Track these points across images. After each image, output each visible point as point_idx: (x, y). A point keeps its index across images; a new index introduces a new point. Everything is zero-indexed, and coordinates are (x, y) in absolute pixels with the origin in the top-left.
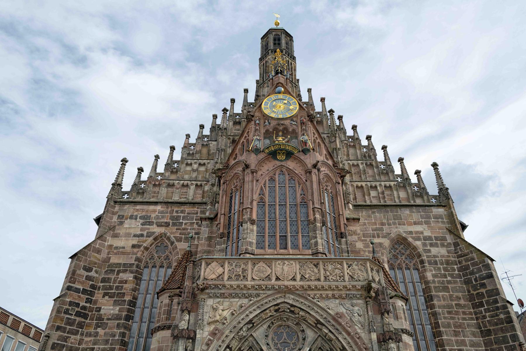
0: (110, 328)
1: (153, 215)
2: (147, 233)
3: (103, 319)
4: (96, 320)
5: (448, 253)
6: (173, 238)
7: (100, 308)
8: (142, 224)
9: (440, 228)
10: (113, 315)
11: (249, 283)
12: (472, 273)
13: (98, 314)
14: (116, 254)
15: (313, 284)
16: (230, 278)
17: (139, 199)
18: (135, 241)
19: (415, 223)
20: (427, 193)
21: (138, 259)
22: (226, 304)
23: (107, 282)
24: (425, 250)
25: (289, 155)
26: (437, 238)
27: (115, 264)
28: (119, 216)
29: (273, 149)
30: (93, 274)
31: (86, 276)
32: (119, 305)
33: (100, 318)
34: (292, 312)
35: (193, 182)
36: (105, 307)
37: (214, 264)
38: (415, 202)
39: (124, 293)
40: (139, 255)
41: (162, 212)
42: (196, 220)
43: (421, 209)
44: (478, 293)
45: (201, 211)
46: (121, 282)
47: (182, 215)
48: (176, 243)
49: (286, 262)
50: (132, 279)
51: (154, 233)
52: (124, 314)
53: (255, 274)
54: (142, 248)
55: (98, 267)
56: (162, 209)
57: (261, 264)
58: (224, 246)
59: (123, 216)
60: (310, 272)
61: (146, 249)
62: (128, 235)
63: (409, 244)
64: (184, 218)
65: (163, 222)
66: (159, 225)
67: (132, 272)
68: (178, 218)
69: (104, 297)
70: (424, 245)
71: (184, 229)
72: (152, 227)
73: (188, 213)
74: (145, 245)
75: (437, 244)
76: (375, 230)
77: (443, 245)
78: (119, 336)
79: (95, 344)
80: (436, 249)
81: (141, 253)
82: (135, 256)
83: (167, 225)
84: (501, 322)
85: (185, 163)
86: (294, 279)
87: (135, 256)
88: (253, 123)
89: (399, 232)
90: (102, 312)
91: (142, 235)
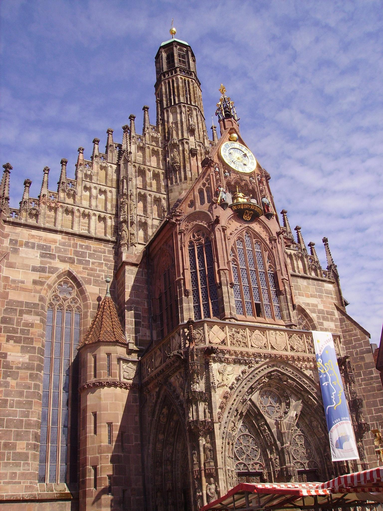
0: (22, 378)
1: (53, 247)
3: (12, 368)
4: (3, 368)
5: (336, 327)
6: (81, 279)
7: (6, 354)
9: (330, 304)
10: (23, 363)
11: (251, 351)
12: (354, 347)
13: (4, 361)
14: (14, 289)
15: (301, 355)
16: (232, 344)
17: (32, 221)
18: (36, 276)
19: (312, 296)
20: (320, 268)
21: (42, 299)
22: (230, 368)
23: (9, 323)
24: (319, 322)
25: (255, 217)
26: (328, 313)
27: (15, 301)
28: (11, 240)
29: (242, 208)
32: (29, 352)
33: (7, 366)
34: (280, 379)
35: (95, 212)
36: (13, 354)
37: (216, 328)
38: (311, 274)
39: (32, 339)
40: (43, 293)
41: (64, 244)
42: (104, 260)
43: (316, 282)
44: (358, 365)
45: (109, 251)
46: (26, 325)
49: (277, 332)
50: (39, 322)
51: (57, 269)
52: (36, 363)
53: (256, 342)
54: (45, 286)
56: (63, 240)
57: (257, 332)
58: (192, 305)
59: (16, 241)
60: (297, 344)
61: (50, 287)
62: (25, 267)
63: (306, 315)
64: (90, 256)
66: (63, 260)
67: (37, 314)
68: (83, 255)
69: (8, 341)
70: (318, 318)
71: (92, 269)
72: (52, 261)
73: (94, 251)
74: (49, 282)
75: (327, 317)
77: (332, 320)
78: (35, 388)
79: (7, 395)
80: (327, 322)
81: (45, 292)
82: (38, 295)
83: (71, 261)
84: (373, 389)
85: (83, 185)
86: (286, 350)
88: (212, 169)
89: (299, 302)
90: (9, 358)
91: (42, 270)
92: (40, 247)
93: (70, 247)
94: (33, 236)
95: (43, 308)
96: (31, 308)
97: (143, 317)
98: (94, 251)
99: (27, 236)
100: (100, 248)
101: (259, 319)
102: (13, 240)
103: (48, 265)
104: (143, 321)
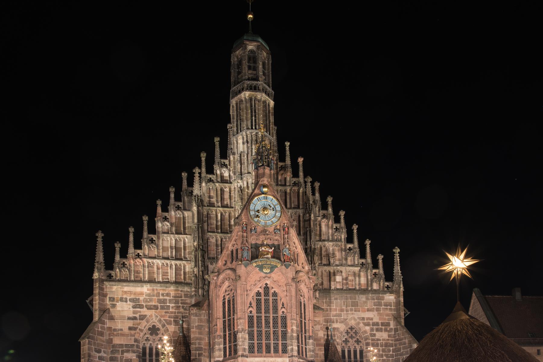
1: (141, 298)
2: (140, 316)
6: (164, 321)
8: (134, 307)
14: (116, 336)
18: (130, 323)
30: (102, 354)
31: (99, 357)
41: (149, 295)
42: (181, 303)
45: (185, 294)
47: (168, 298)
48: (167, 326)
51: (145, 316)
54: (138, 330)
55: (105, 348)
59: (114, 298)
61: (141, 330)
64: (170, 301)
65: (151, 305)
66: (149, 308)
68: (164, 301)
71: (172, 313)
76: (335, 316)
82: (133, 338)
83: (156, 308)
87: (133, 338)
92: (132, 300)
93: (154, 296)
94: (126, 292)
95: (138, 347)
96: (128, 348)
97: (205, 349)
98: (173, 297)
99: (121, 293)
100: (178, 294)
101: (268, 355)
102: (112, 298)
103: (139, 314)
104: (204, 352)
